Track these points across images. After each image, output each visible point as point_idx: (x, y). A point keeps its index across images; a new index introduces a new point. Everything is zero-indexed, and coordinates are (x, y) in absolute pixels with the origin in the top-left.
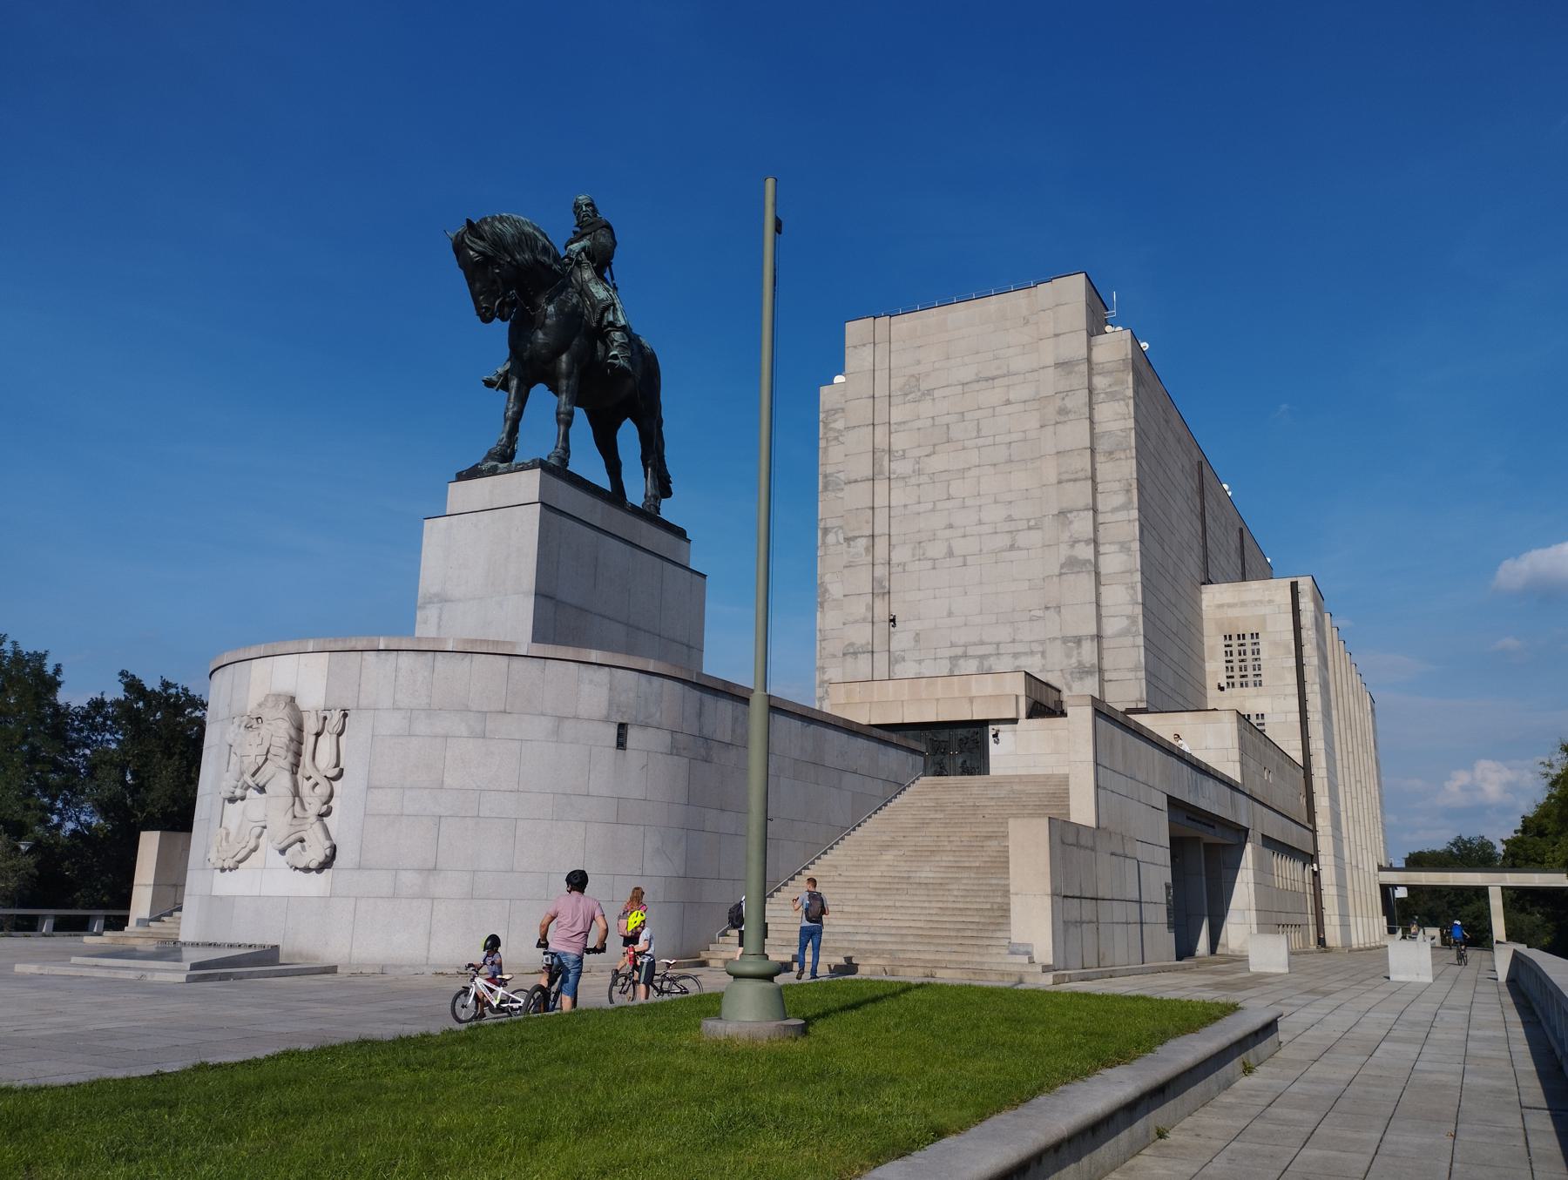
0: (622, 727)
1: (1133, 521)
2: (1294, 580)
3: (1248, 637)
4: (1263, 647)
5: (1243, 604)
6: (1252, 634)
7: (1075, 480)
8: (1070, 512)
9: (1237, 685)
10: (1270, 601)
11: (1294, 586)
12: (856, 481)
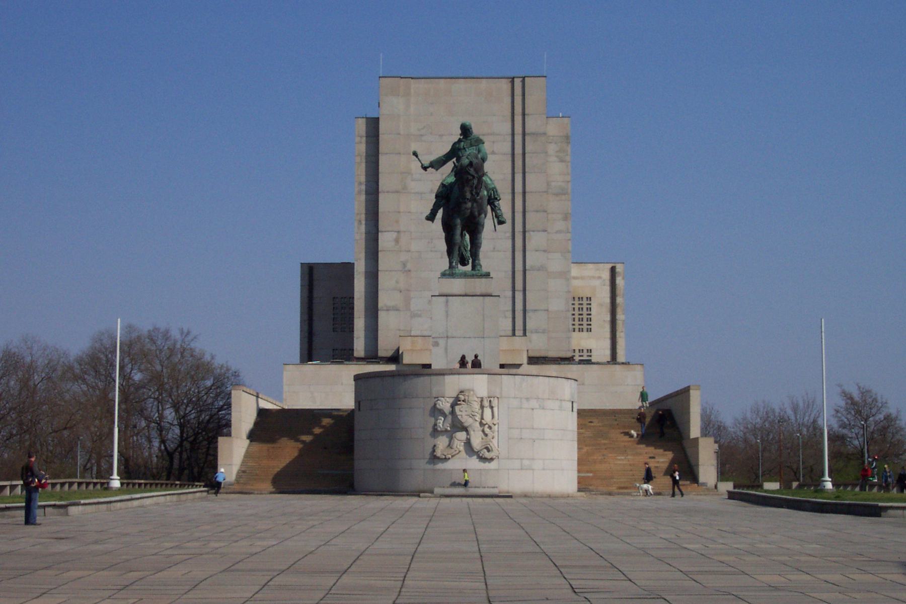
0: (572, 402)
1: (569, 240)
2: (613, 265)
3: (585, 299)
4: (593, 306)
5: (582, 278)
6: (587, 298)
7: (537, 211)
8: (533, 231)
9: (577, 330)
10: (600, 278)
11: (613, 270)
12: (388, 192)
